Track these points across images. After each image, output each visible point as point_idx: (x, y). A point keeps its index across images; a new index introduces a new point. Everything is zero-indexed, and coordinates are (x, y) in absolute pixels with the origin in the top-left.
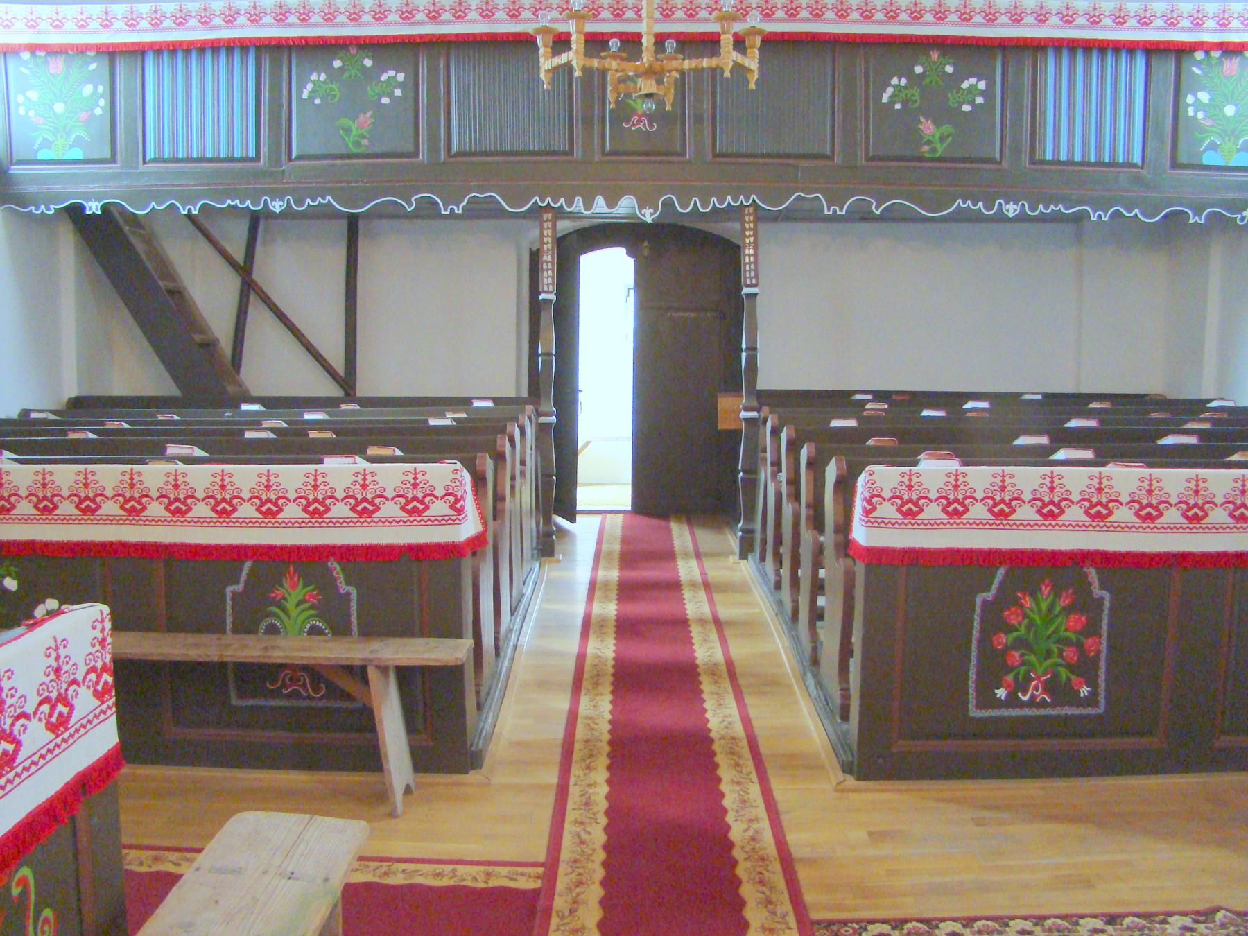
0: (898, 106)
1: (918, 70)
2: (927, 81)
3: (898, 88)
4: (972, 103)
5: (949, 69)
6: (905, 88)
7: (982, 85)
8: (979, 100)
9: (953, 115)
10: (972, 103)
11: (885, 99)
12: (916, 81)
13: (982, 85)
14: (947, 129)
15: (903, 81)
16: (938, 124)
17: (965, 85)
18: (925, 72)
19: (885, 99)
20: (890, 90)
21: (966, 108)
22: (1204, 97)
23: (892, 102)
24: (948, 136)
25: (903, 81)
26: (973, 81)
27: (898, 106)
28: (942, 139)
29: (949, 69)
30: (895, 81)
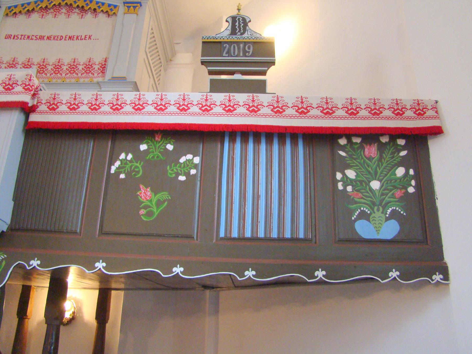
0: (122, 176)
1: (143, 147)
2: (150, 156)
3: (124, 162)
4: (187, 174)
5: (170, 147)
6: (131, 161)
7: (197, 160)
8: (193, 172)
9: (169, 184)
10: (187, 174)
11: (113, 169)
12: (138, 156)
13: (197, 160)
14: (164, 195)
15: (130, 157)
16: (155, 192)
17: (182, 160)
18: (149, 149)
19: (113, 169)
20: (118, 164)
21: (182, 178)
22: (351, 174)
23: (118, 173)
24: (165, 201)
25: (130, 157)
26: (189, 157)
27: (122, 176)
28: (159, 203)
29: (170, 147)
30: (123, 156)
